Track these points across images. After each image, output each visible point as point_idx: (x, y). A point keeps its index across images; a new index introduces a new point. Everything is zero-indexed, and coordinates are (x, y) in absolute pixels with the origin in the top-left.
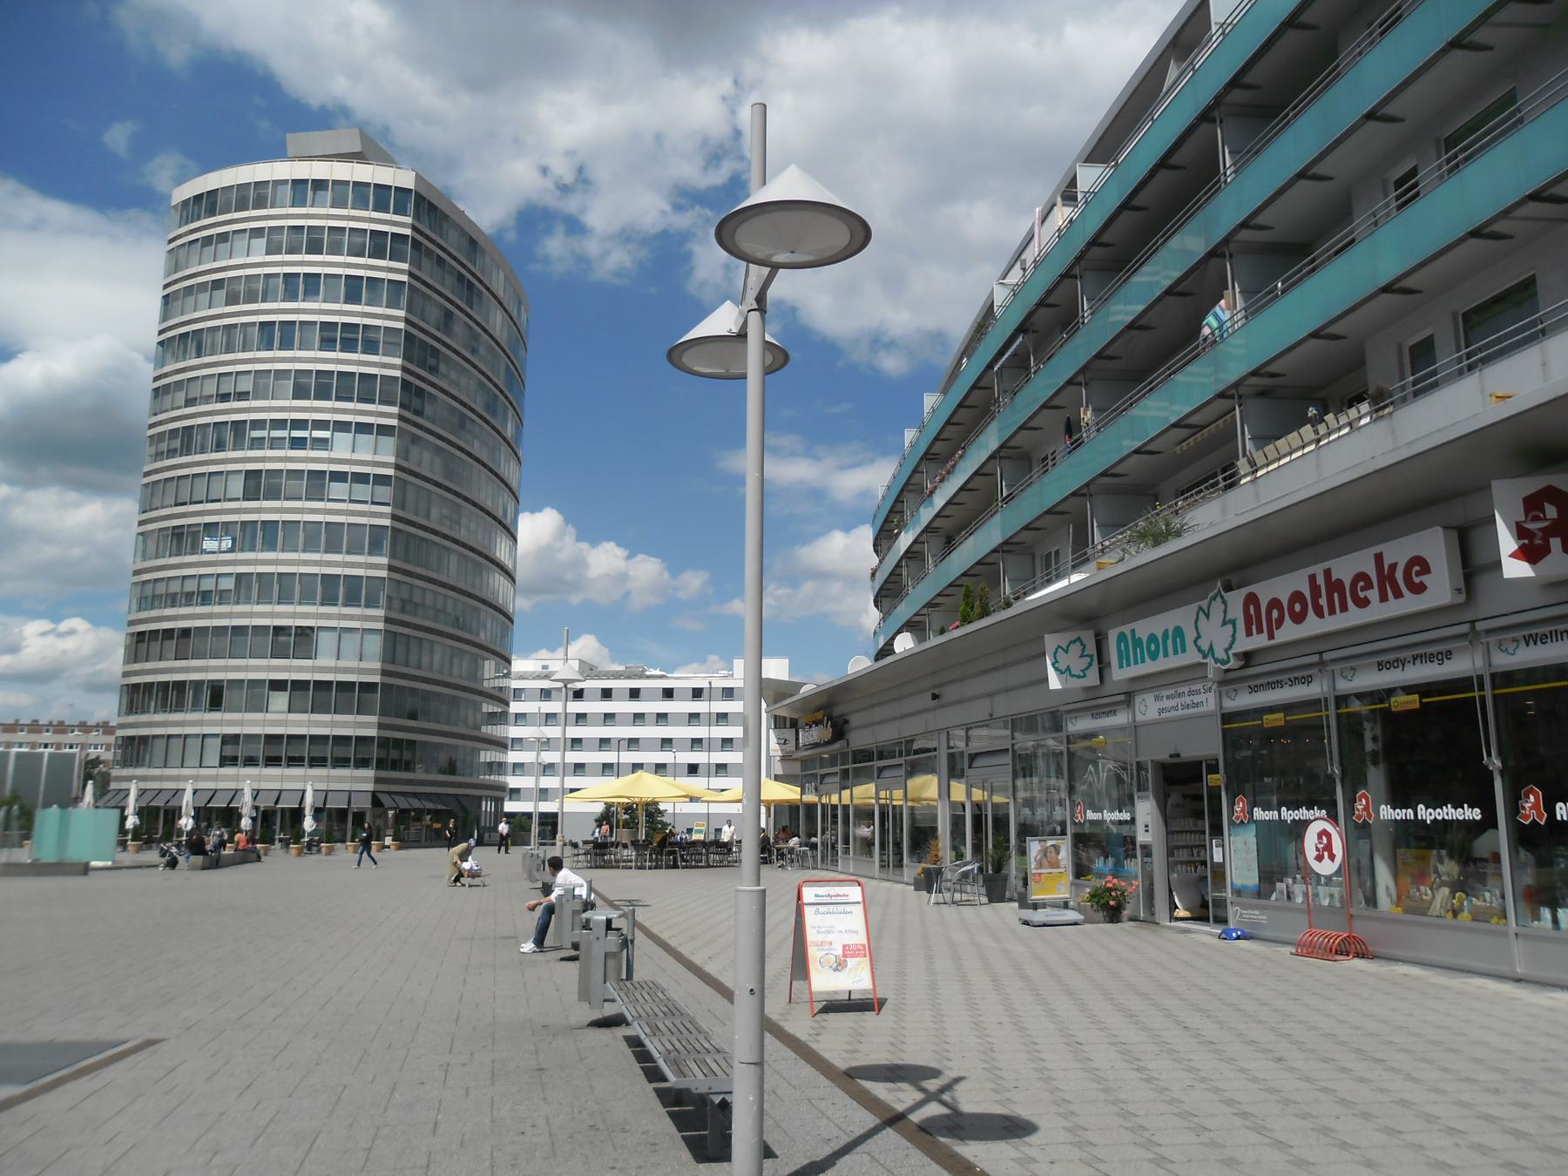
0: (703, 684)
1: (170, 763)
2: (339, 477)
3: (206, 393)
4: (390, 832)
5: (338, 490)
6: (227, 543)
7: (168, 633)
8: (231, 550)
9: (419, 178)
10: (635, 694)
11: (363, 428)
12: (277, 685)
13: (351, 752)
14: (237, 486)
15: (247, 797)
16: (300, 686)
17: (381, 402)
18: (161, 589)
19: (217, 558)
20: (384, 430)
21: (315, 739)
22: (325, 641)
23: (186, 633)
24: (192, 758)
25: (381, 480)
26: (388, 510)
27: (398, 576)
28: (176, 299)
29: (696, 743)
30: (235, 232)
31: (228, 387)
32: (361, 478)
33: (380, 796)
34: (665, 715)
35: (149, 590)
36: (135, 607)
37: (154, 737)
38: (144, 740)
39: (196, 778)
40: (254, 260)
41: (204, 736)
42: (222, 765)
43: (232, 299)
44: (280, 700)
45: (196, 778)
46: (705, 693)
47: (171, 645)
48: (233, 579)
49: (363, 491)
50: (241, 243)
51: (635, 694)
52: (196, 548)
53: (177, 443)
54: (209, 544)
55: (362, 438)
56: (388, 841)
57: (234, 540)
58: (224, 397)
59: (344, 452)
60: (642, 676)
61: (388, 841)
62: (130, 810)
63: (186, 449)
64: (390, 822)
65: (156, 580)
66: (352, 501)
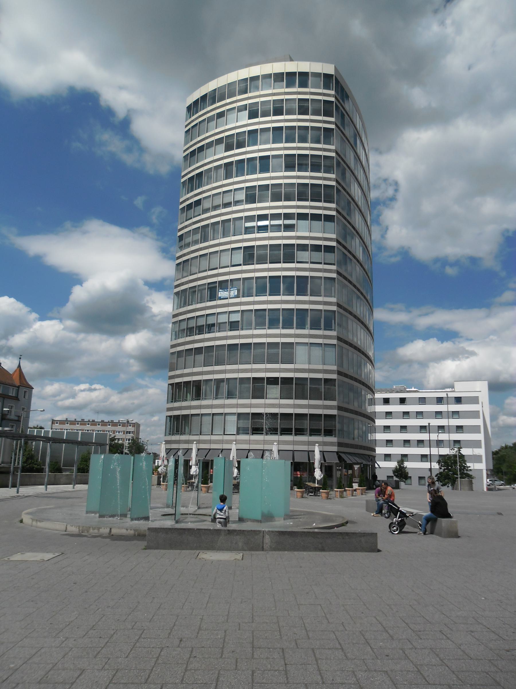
0: (444, 395)
1: (193, 433)
2: (303, 248)
3: (215, 204)
4: (357, 480)
5: (305, 255)
6: (234, 292)
7: (199, 351)
8: (237, 296)
9: (336, 69)
10: (403, 401)
11: (316, 217)
12: (273, 381)
13: (322, 425)
14: (239, 257)
15: (317, 456)
16: (287, 381)
17: (325, 201)
18: (192, 324)
19: (230, 304)
20: (329, 218)
21: (299, 416)
22: (301, 353)
23: (210, 348)
24: (218, 430)
25: (329, 249)
26: (334, 267)
27: (341, 311)
28: (213, 120)
29: (441, 428)
30: (228, 110)
31: (229, 198)
32: (317, 248)
33: (343, 456)
34: (421, 413)
35: (184, 326)
36: (174, 337)
37: (192, 415)
38: (186, 417)
39: (199, 442)
40: (242, 123)
41: (213, 414)
42: (238, 433)
43: (229, 148)
44: (275, 390)
45: (199, 442)
46: (445, 400)
47: (200, 358)
48: (240, 314)
49: (319, 256)
50: (232, 116)
51: (403, 401)
52: (213, 296)
53: (198, 236)
54: (222, 294)
55: (315, 223)
56: (355, 486)
57: (239, 291)
58: (227, 205)
59: (304, 233)
60: (392, 391)
61: (355, 486)
62: (193, 462)
63: (205, 239)
64: (356, 473)
65: (188, 319)
66: (312, 263)
